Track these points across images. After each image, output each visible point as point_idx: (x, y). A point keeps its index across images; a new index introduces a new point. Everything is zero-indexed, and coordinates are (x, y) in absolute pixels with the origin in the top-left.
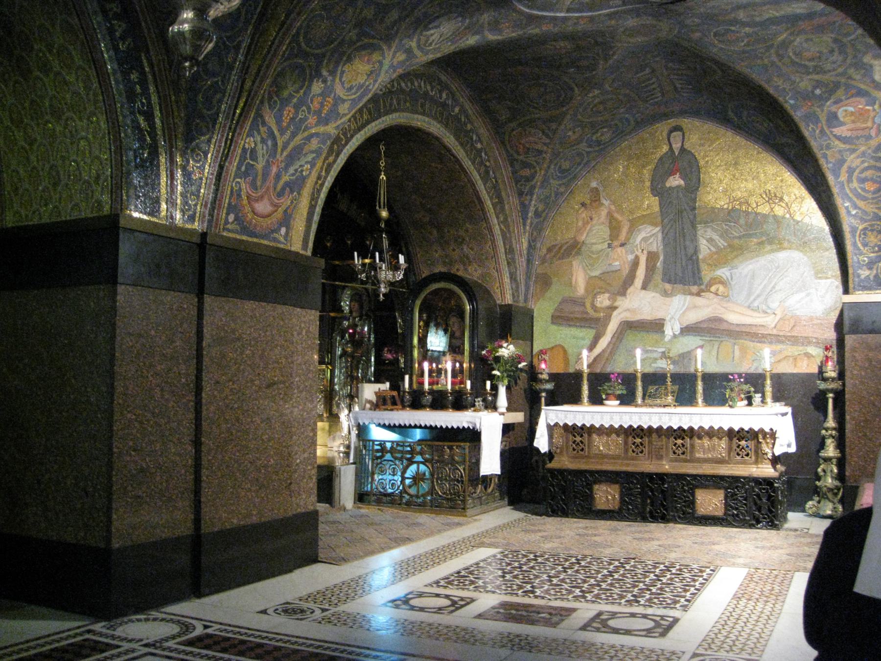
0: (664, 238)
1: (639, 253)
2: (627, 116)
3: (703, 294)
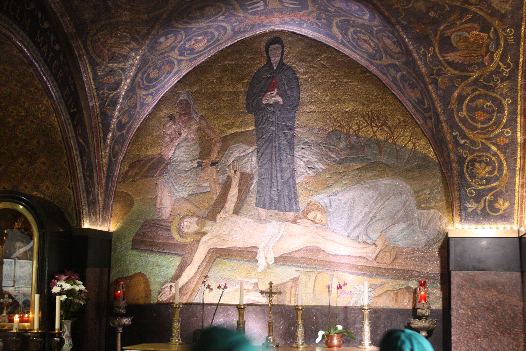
0: (259, 160)
2: (224, 24)
3: (299, 221)
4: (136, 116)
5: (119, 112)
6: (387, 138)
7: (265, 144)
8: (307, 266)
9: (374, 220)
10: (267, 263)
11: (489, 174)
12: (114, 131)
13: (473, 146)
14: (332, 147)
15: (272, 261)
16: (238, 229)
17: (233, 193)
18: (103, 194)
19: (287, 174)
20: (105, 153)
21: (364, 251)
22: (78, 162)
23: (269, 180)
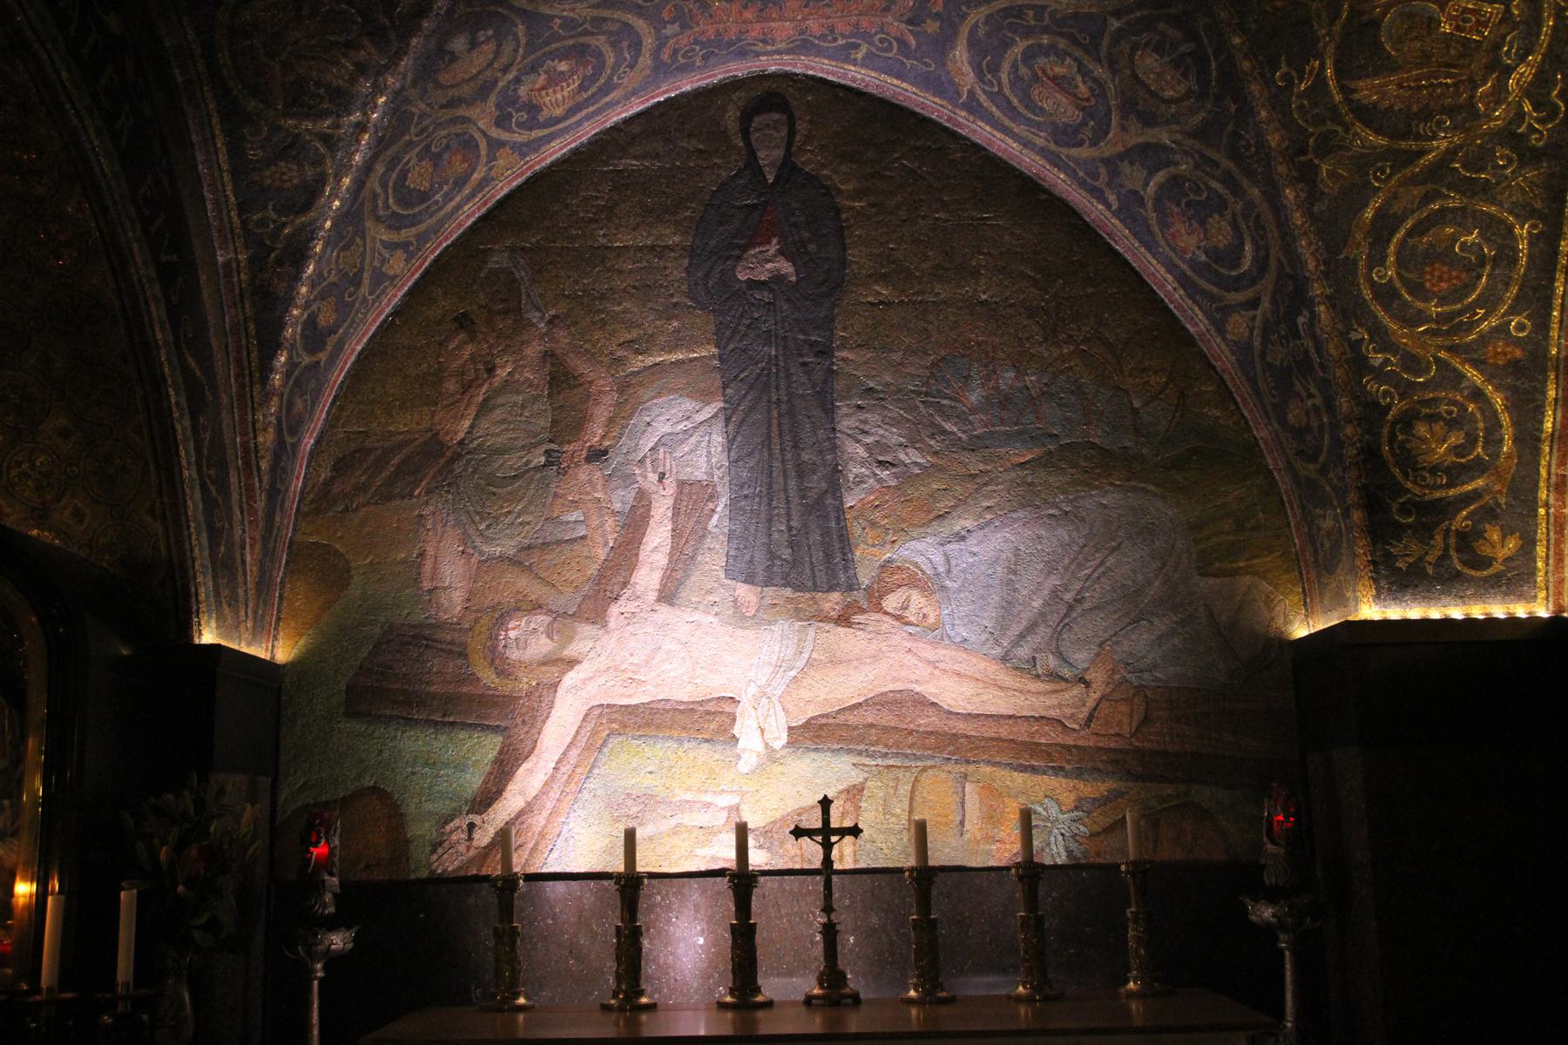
3: (858, 618)
4: (357, 312)
5: (313, 286)
7: (749, 397)
8: (885, 750)
9: (1079, 609)
10: (766, 744)
11: (1458, 455)
12: (293, 346)
13: (1407, 369)
14: (945, 402)
15: (780, 739)
16: (674, 646)
17: (658, 539)
18: (258, 546)
19: (816, 483)
20: (265, 416)
21: (1052, 700)
22: (184, 429)
23: (765, 500)
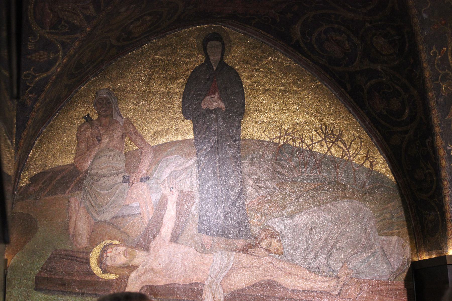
1: (166, 191)
3: (250, 250)
6: (342, 155)
